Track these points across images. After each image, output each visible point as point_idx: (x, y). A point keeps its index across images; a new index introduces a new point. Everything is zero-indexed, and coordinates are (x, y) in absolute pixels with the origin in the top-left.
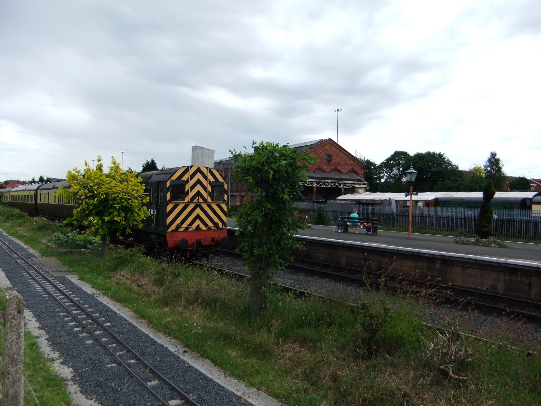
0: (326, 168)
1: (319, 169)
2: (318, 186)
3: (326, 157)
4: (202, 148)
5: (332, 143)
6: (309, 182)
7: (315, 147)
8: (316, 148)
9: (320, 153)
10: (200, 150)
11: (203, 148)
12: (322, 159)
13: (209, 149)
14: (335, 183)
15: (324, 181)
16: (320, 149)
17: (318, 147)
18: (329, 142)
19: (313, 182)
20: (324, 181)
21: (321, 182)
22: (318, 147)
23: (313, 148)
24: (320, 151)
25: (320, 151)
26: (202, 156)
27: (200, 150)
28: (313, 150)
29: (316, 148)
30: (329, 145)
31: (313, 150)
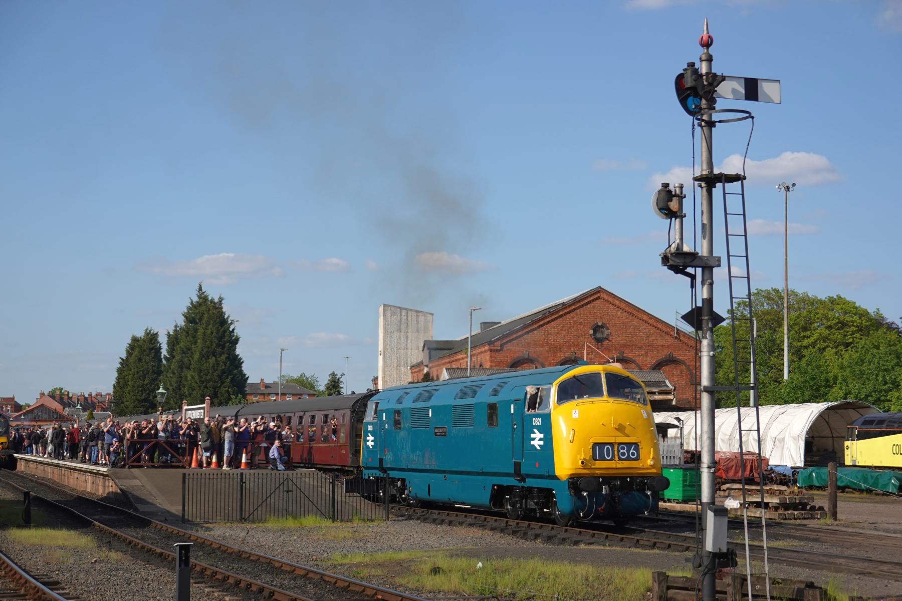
3: (591, 332)
9: (575, 322)
16: (573, 314)
24: (573, 318)
25: (574, 317)
28: (553, 317)
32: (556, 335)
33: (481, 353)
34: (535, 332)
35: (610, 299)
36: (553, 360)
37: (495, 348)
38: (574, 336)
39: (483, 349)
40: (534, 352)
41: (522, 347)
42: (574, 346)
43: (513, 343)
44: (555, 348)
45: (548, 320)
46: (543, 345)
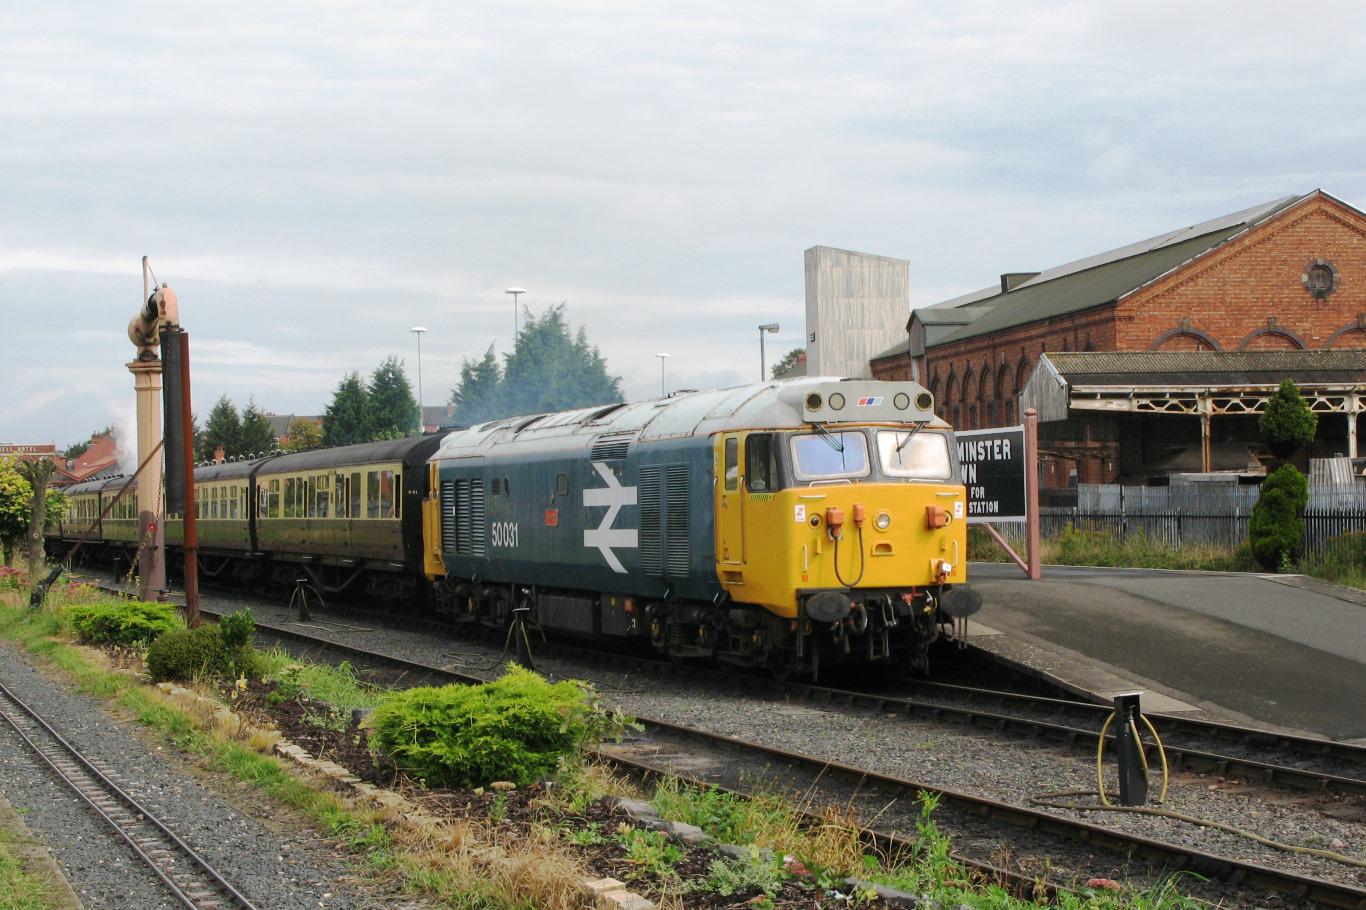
0: (1307, 325)
1: (1271, 334)
2: (1223, 411)
4: (843, 257)
5: (1330, 210)
6: (1173, 395)
7: (1241, 239)
8: (1247, 242)
9: (1273, 261)
10: (837, 263)
11: (850, 254)
12: (1281, 288)
13: (879, 258)
14: (1312, 393)
15: (1248, 387)
16: (1269, 245)
17: (1256, 237)
18: (1314, 206)
19: (1192, 395)
20: (1248, 387)
21: (1237, 395)
22: (1256, 237)
23: (1232, 244)
24: (1271, 250)
25: (1271, 250)
26: (849, 293)
27: (837, 263)
28: (1233, 251)
29: (1247, 242)
30: (1316, 222)
31: (1233, 251)
32: (1239, 286)
33: (1089, 324)
34: (1200, 281)
35: (1338, 214)
36: (1235, 333)
37: (1126, 314)
38: (1273, 286)
39: (1097, 317)
40: (1199, 321)
41: (1176, 310)
42: (1273, 306)
43: (1160, 303)
44: (1238, 310)
45: (1223, 256)
46: (1216, 306)
